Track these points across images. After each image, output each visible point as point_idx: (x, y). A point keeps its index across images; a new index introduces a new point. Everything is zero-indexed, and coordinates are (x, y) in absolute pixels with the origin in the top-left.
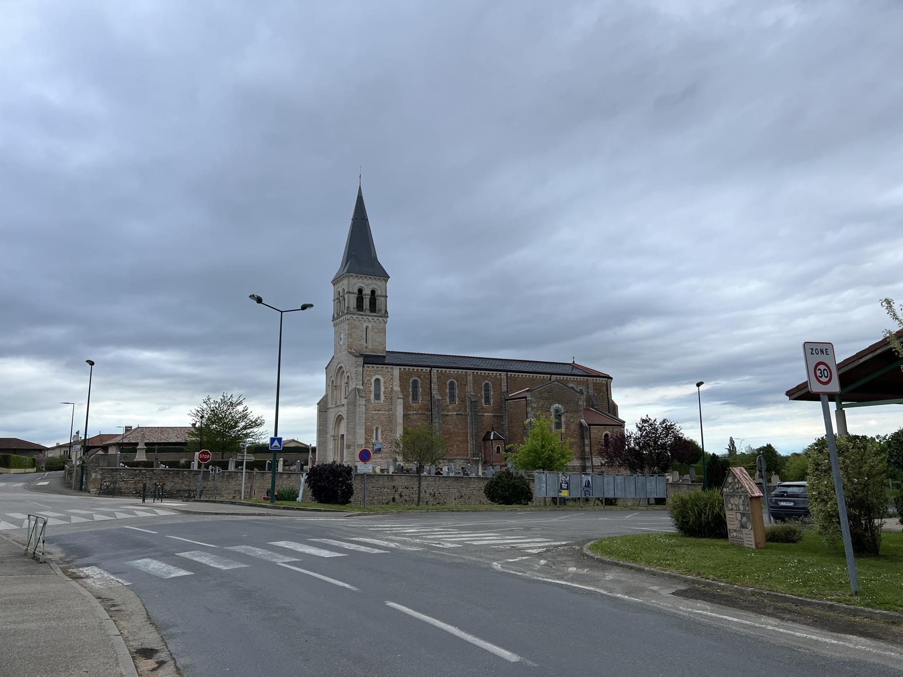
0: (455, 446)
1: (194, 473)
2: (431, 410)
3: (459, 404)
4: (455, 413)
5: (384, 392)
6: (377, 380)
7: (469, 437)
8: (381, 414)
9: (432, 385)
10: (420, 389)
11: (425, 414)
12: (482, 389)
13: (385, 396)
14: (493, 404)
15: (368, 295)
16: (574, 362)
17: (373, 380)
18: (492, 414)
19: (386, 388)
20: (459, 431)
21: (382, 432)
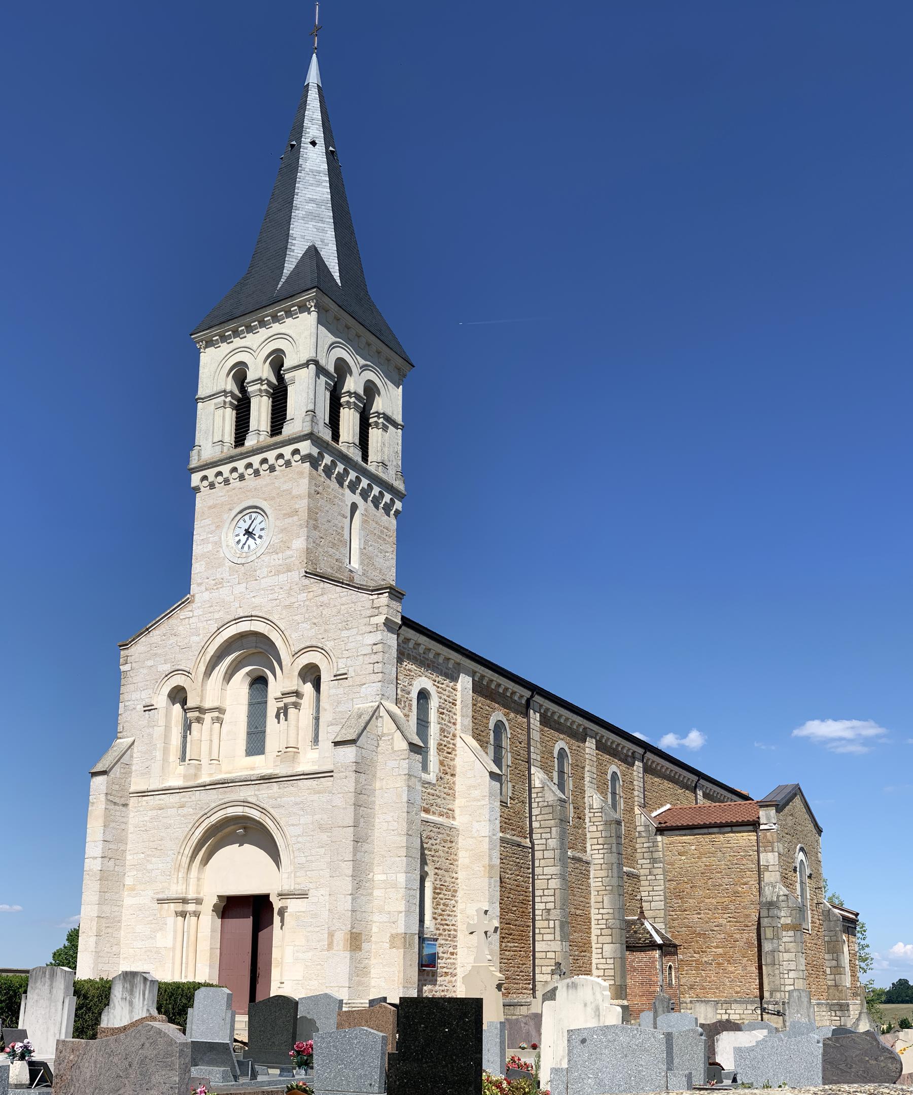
2: (531, 833)
5: (440, 748)
6: (423, 695)
7: (595, 931)
8: (436, 825)
9: (532, 749)
11: (519, 845)
13: (442, 763)
17: (414, 695)
19: (442, 730)
20: (578, 912)
21: (436, 892)
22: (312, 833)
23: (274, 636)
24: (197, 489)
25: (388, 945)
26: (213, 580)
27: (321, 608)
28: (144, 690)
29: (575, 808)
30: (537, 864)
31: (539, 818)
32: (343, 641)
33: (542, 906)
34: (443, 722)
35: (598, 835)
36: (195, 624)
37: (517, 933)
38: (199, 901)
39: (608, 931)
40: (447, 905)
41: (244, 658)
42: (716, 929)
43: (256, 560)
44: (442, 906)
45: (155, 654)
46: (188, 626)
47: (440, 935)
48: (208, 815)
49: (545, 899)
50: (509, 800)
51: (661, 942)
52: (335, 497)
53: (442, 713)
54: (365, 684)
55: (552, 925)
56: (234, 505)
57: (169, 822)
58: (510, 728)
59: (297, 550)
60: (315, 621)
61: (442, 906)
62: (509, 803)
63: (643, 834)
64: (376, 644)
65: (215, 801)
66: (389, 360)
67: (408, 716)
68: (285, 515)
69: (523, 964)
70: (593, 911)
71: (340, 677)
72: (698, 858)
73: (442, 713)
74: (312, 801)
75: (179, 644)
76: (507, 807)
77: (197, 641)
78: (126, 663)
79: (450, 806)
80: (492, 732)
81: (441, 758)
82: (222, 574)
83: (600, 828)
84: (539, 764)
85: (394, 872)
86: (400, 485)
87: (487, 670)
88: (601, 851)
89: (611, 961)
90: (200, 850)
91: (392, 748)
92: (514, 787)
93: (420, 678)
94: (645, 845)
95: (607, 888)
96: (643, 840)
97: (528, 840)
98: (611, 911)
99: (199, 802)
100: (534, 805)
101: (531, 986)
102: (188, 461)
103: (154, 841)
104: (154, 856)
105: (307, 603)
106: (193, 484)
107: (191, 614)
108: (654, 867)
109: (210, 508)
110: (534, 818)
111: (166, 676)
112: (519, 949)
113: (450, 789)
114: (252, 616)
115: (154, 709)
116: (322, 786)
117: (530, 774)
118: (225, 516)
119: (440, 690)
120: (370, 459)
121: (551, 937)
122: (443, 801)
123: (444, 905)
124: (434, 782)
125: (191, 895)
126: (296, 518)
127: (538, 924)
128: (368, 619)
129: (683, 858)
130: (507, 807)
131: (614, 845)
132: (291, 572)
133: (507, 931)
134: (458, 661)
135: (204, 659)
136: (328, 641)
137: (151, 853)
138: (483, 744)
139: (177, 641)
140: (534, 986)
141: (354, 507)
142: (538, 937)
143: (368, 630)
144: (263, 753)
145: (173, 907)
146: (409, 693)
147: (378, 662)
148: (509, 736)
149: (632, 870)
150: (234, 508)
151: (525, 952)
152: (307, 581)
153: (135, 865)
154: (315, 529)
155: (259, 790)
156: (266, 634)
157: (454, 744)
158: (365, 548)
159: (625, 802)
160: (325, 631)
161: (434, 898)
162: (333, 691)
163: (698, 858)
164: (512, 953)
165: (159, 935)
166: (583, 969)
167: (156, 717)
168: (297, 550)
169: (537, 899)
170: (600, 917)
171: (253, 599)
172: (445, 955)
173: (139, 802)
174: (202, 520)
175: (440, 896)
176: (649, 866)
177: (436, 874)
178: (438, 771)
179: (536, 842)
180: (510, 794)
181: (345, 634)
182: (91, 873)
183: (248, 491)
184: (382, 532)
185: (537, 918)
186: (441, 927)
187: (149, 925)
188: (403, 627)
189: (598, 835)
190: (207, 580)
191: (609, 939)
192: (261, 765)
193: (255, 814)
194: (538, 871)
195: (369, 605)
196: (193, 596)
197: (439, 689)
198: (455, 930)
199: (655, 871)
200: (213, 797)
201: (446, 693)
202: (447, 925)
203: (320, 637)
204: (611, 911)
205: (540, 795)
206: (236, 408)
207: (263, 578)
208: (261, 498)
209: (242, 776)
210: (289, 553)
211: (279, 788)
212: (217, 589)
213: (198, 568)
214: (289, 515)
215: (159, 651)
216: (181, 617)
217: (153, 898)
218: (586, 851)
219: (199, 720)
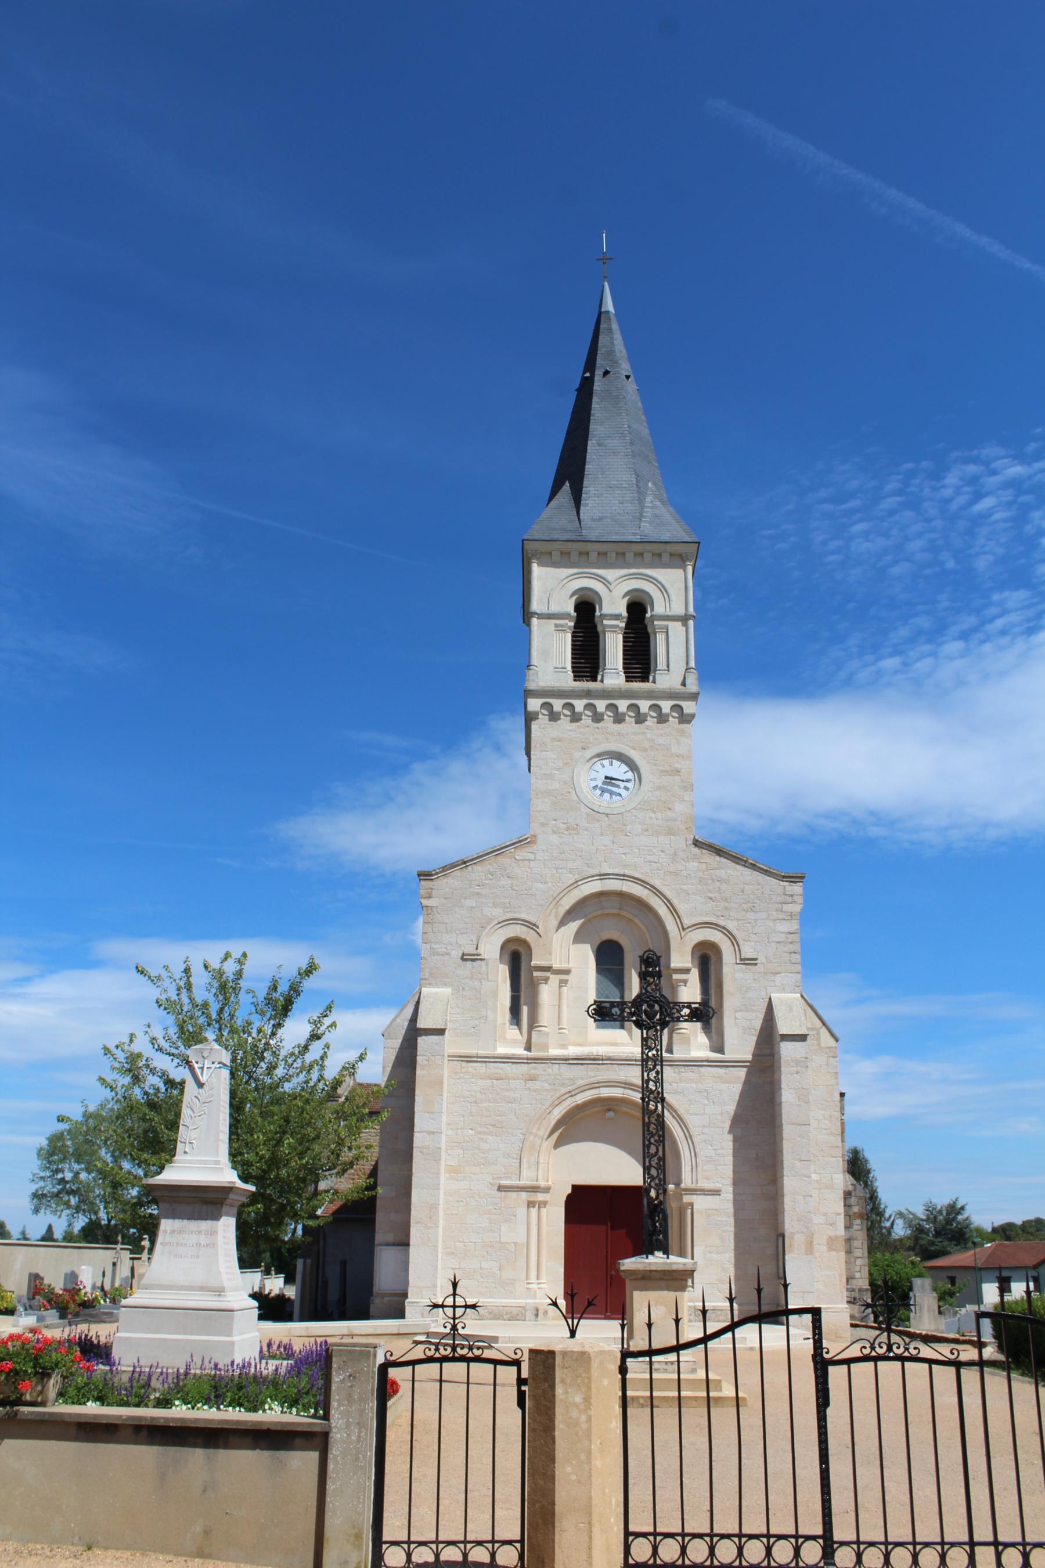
22: (722, 1125)
25: (825, 1248)
26: (564, 824)
27: (718, 883)
28: (462, 934)
32: (749, 923)
36: (539, 869)
38: (547, 1190)
41: (595, 917)
43: (626, 814)
45: (478, 894)
46: (528, 870)
48: (573, 1093)
54: (780, 973)
56: (590, 745)
57: (513, 1095)
59: (682, 815)
60: (712, 895)
64: (792, 933)
65: (582, 1079)
68: (662, 771)
71: (749, 962)
74: (720, 1090)
75: (516, 888)
78: (430, 897)
82: (575, 819)
85: (828, 1172)
91: (819, 1044)
99: (559, 1077)
102: (523, 678)
103: (490, 1116)
104: (490, 1134)
105: (700, 874)
107: (532, 857)
109: (553, 740)
111: (499, 923)
114: (624, 875)
115: (481, 960)
116: (731, 1075)
118: (577, 754)
125: (542, 1183)
126: (677, 778)
128: (780, 905)
132: (674, 835)
135: (557, 912)
136: (730, 920)
137: (485, 1130)
139: (512, 884)
143: (781, 917)
145: (524, 1195)
147: (795, 953)
150: (588, 748)
152: (696, 850)
153: (459, 1143)
160: (726, 908)
162: (739, 975)
165: (504, 1228)
167: (484, 968)
168: (682, 815)
171: (624, 856)
173: (462, 1067)
174: (542, 751)
181: (751, 916)
182: (425, 1151)
183: (610, 734)
187: (488, 1216)
190: (555, 822)
195: (780, 891)
196: (534, 836)
200: (583, 1075)
203: (719, 913)
207: (636, 835)
208: (628, 746)
209: (623, 1053)
210: (669, 814)
211: (675, 1072)
212: (570, 834)
215: (484, 891)
216: (517, 857)
217: (492, 1185)
219: (546, 980)
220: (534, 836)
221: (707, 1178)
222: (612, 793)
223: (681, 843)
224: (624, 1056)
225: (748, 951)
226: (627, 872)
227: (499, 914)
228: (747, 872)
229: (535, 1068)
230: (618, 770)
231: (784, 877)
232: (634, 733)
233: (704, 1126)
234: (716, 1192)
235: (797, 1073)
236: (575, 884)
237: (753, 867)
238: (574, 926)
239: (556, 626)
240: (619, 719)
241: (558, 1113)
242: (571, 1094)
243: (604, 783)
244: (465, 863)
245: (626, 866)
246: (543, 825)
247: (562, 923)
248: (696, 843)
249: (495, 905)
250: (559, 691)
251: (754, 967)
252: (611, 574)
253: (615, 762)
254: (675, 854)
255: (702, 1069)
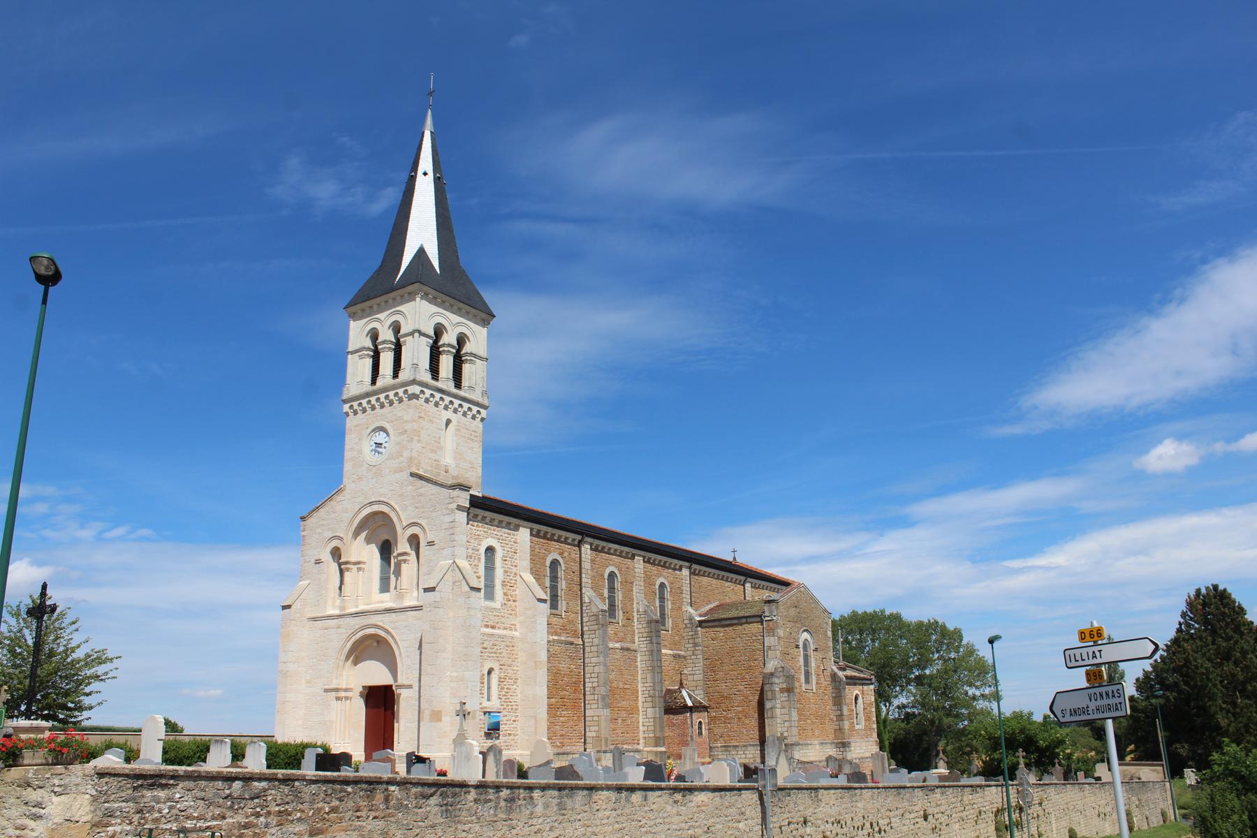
0: (620, 721)
1: (419, 789)
2: (582, 635)
3: (624, 626)
4: (618, 645)
5: (504, 584)
6: (490, 550)
7: (641, 699)
8: (499, 636)
9: (583, 576)
10: (564, 582)
11: (572, 644)
12: (655, 594)
13: (505, 594)
14: (672, 630)
15: (449, 345)
16: (735, 558)
17: (483, 551)
18: (671, 652)
20: (626, 687)
21: (501, 681)
23: (393, 515)
24: (347, 414)
29: (624, 613)
30: (586, 656)
31: (588, 624)
33: (590, 685)
34: (506, 566)
35: (643, 630)
37: (570, 704)
39: (650, 699)
40: (510, 689)
42: (736, 693)
44: (505, 690)
47: (504, 709)
49: (592, 680)
50: (563, 613)
51: (692, 705)
52: (434, 417)
53: (505, 560)
55: (596, 698)
58: (564, 563)
61: (505, 690)
62: (563, 615)
63: (689, 626)
66: (475, 316)
67: (478, 566)
69: (575, 726)
70: (640, 685)
71: (431, 544)
72: (725, 642)
73: (505, 560)
76: (563, 618)
77: (349, 515)
79: (513, 622)
80: (548, 568)
81: (505, 591)
83: (644, 626)
84: (590, 585)
86: (486, 402)
87: (541, 526)
88: (645, 642)
89: (652, 720)
90: (350, 658)
91: (461, 591)
92: (568, 603)
93: (488, 540)
94: (690, 634)
95: (649, 668)
96: (688, 630)
97: (580, 639)
98: (652, 685)
100: (585, 615)
101: (583, 740)
102: (341, 394)
106: (345, 411)
107: (343, 498)
108: (696, 650)
109: (355, 426)
110: (584, 624)
112: (572, 715)
113: (512, 610)
117: (581, 594)
119: (503, 545)
120: (465, 383)
121: (595, 706)
122: (507, 620)
123: (507, 689)
124: (499, 607)
126: (406, 436)
127: (587, 698)
129: (715, 642)
130: (563, 618)
131: (654, 638)
133: (561, 704)
134: (517, 523)
138: (538, 578)
140: (585, 740)
141: (448, 422)
142: (587, 706)
144: (389, 591)
146: (478, 550)
148: (563, 568)
149: (677, 652)
151: (578, 717)
152: (412, 479)
154: (418, 442)
155: (384, 617)
156: (388, 513)
157: (515, 580)
158: (457, 449)
159: (672, 603)
161: (499, 685)
162: (427, 553)
163: (725, 642)
164: (566, 718)
166: (631, 726)
169: (587, 680)
170: (645, 689)
172: (509, 722)
175: (504, 683)
176: (693, 649)
177: (501, 669)
178: (502, 600)
179: (586, 640)
180: (564, 609)
181: (434, 514)
184: (471, 435)
185: (587, 693)
186: (506, 704)
188: (472, 508)
189: (643, 630)
191: (650, 705)
192: (387, 600)
193: (382, 633)
194: (587, 660)
196: (345, 486)
197: (503, 545)
198: (517, 705)
199: (696, 653)
201: (509, 546)
202: (510, 702)
203: (419, 516)
204: (652, 685)
205: (588, 608)
206: (373, 357)
210: (401, 459)
213: (348, 467)
214: (401, 434)
218: (635, 643)
220: (345, 486)
221: (407, 678)
222: (379, 453)
223: (406, 475)
224: (374, 609)
225: (430, 537)
226: (381, 499)
227: (330, 534)
228: (434, 487)
229: (340, 621)
230: (381, 437)
231: (450, 487)
232: (390, 412)
233: (407, 647)
234: (410, 687)
235: (430, 611)
236: (359, 511)
237: (436, 483)
238: (364, 535)
239: (359, 356)
240: (382, 406)
241: (349, 645)
242: (354, 634)
243: (376, 447)
244: (317, 508)
245: (381, 496)
246: (349, 478)
247: (356, 534)
248: (412, 475)
249: (329, 530)
250: (360, 395)
251: (432, 547)
252: (381, 316)
253: (381, 432)
254: (402, 483)
255: (407, 613)
